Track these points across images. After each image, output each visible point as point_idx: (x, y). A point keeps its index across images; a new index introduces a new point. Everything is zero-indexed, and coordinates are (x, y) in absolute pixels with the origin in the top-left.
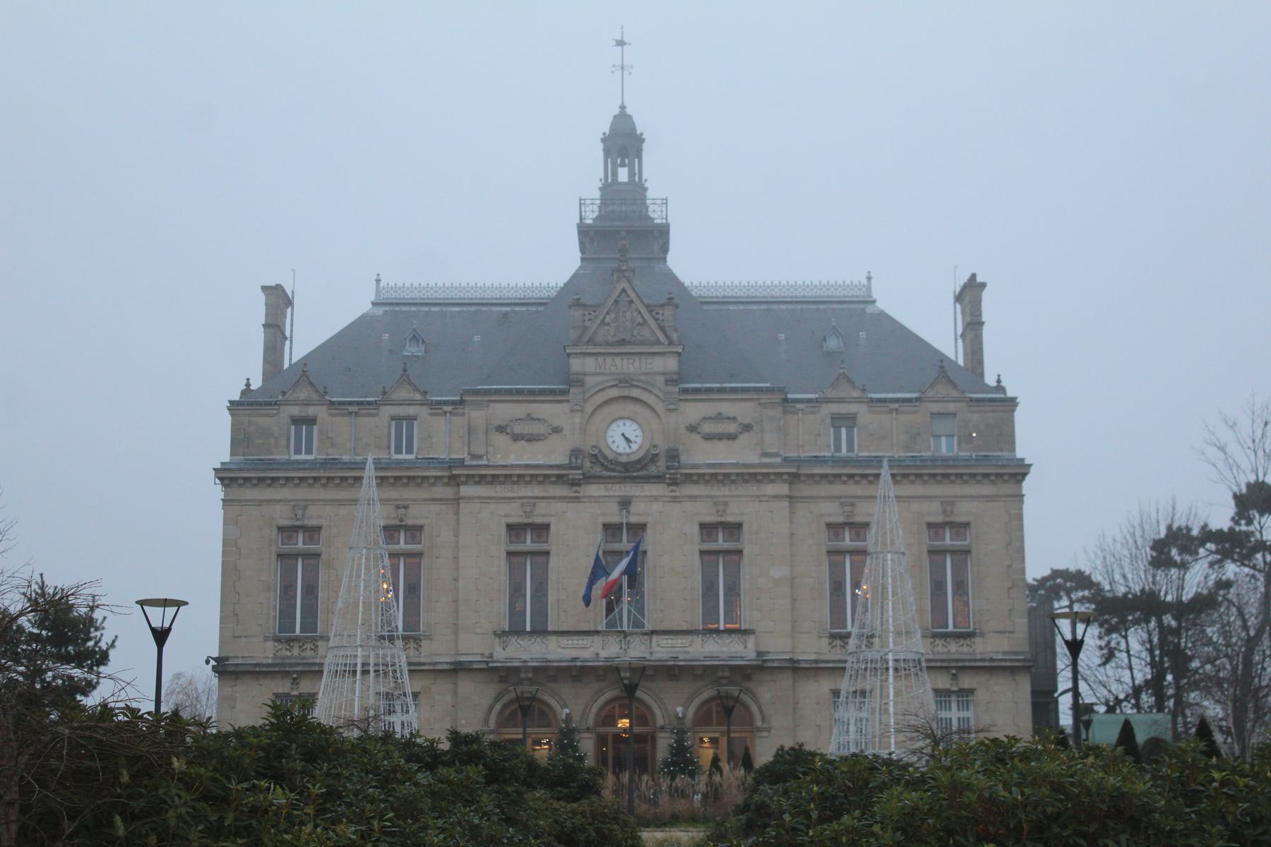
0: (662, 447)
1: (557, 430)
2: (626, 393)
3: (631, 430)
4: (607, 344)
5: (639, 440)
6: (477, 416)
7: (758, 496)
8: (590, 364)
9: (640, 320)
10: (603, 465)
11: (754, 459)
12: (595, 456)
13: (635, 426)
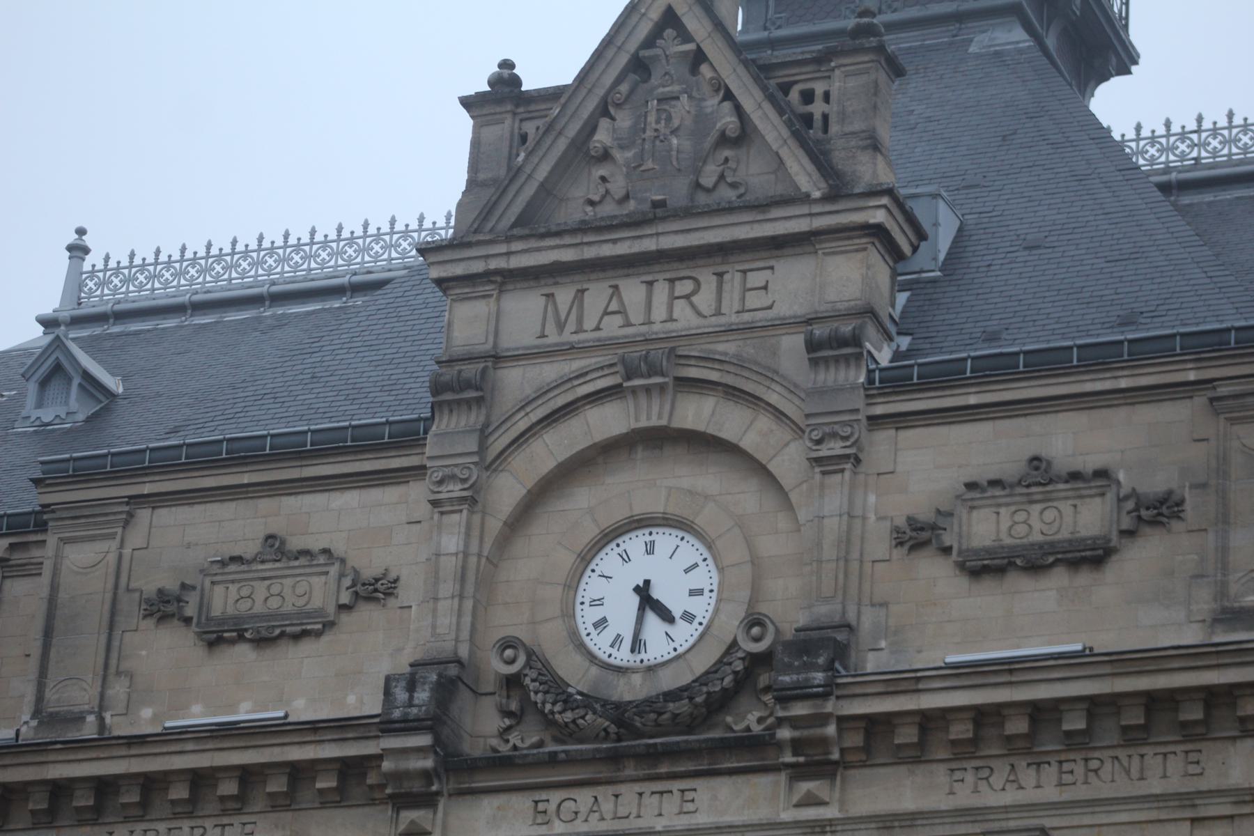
0: (790, 612)
1: (375, 591)
2: (652, 415)
3: (678, 569)
4: (584, 228)
5: (702, 608)
6: (82, 562)
7: (1186, 799)
8: (523, 317)
9: (728, 120)
10: (548, 721)
11: (1191, 636)
12: (512, 683)
13: (691, 551)
